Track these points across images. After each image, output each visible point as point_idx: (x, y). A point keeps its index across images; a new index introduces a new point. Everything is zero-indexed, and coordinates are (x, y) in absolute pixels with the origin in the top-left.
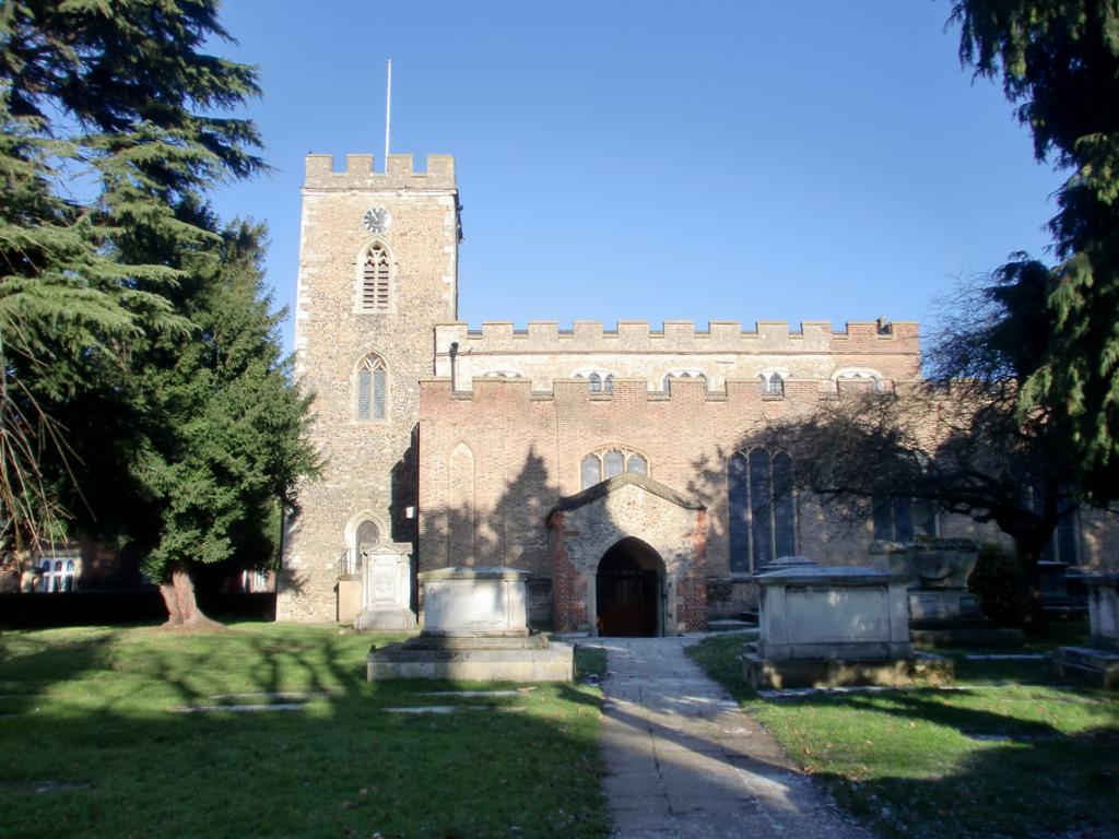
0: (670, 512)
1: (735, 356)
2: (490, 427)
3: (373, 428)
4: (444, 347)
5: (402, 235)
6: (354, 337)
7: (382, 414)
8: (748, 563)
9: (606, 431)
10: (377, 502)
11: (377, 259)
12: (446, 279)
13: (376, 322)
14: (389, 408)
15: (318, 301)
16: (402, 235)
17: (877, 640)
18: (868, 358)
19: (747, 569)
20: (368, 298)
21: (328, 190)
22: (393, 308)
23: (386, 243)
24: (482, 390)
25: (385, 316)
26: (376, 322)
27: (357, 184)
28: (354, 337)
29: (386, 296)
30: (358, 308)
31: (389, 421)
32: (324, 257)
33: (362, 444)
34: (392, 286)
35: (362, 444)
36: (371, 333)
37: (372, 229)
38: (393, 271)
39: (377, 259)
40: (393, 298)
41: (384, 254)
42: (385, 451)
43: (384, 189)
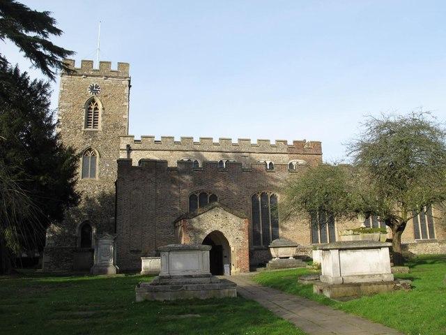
0: (233, 219)
1: (248, 154)
4: (123, 146)
6: (82, 141)
7: (93, 175)
8: (260, 242)
9: (201, 184)
11: (93, 107)
14: (97, 173)
17: (377, 273)
18: (302, 156)
19: (260, 244)
20: (87, 125)
23: (97, 100)
25: (97, 132)
28: (82, 141)
31: (97, 178)
32: (69, 104)
34: (100, 119)
38: (100, 112)
39: (93, 107)
41: (97, 104)
43: (98, 76)
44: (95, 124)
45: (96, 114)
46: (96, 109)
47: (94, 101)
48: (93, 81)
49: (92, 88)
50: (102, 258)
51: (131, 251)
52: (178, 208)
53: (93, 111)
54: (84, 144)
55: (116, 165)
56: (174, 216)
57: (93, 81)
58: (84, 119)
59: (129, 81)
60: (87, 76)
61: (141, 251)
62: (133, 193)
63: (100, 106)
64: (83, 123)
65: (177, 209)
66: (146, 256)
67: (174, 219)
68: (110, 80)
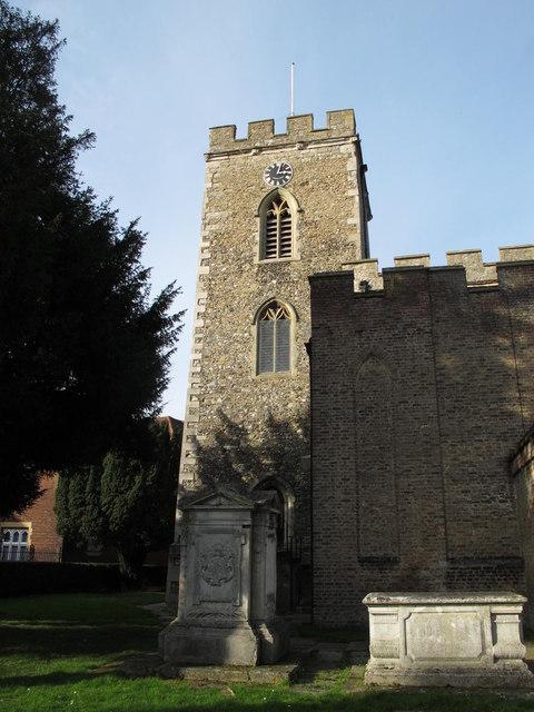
2: (410, 330)
3: (276, 381)
5: (303, 185)
6: (254, 287)
10: (281, 464)
11: (277, 211)
12: (350, 221)
13: (277, 270)
15: (219, 255)
16: (303, 185)
20: (266, 251)
21: (229, 154)
22: (295, 254)
23: (287, 196)
24: (396, 283)
26: (277, 270)
27: (258, 144)
28: (254, 287)
29: (290, 245)
30: (256, 260)
32: (226, 214)
33: (265, 399)
35: (265, 399)
36: (274, 282)
37: (273, 182)
38: (295, 219)
39: (277, 211)
40: (295, 244)
41: (286, 205)
42: (290, 405)
43: (284, 146)
44: (285, 248)
45: (285, 227)
46: (286, 215)
47: (278, 200)
48: (274, 158)
49: (273, 173)
50: (205, 586)
51: (362, 561)
52: (517, 409)
53: (277, 221)
54: (260, 293)
55: (306, 287)
56: (503, 437)
57: (274, 158)
58: (258, 239)
59: (357, 144)
60: (260, 149)
61: (395, 561)
62: (363, 369)
63: (293, 208)
64: (256, 249)
65: (511, 415)
66: (411, 583)
67: (504, 448)
68: (312, 150)
